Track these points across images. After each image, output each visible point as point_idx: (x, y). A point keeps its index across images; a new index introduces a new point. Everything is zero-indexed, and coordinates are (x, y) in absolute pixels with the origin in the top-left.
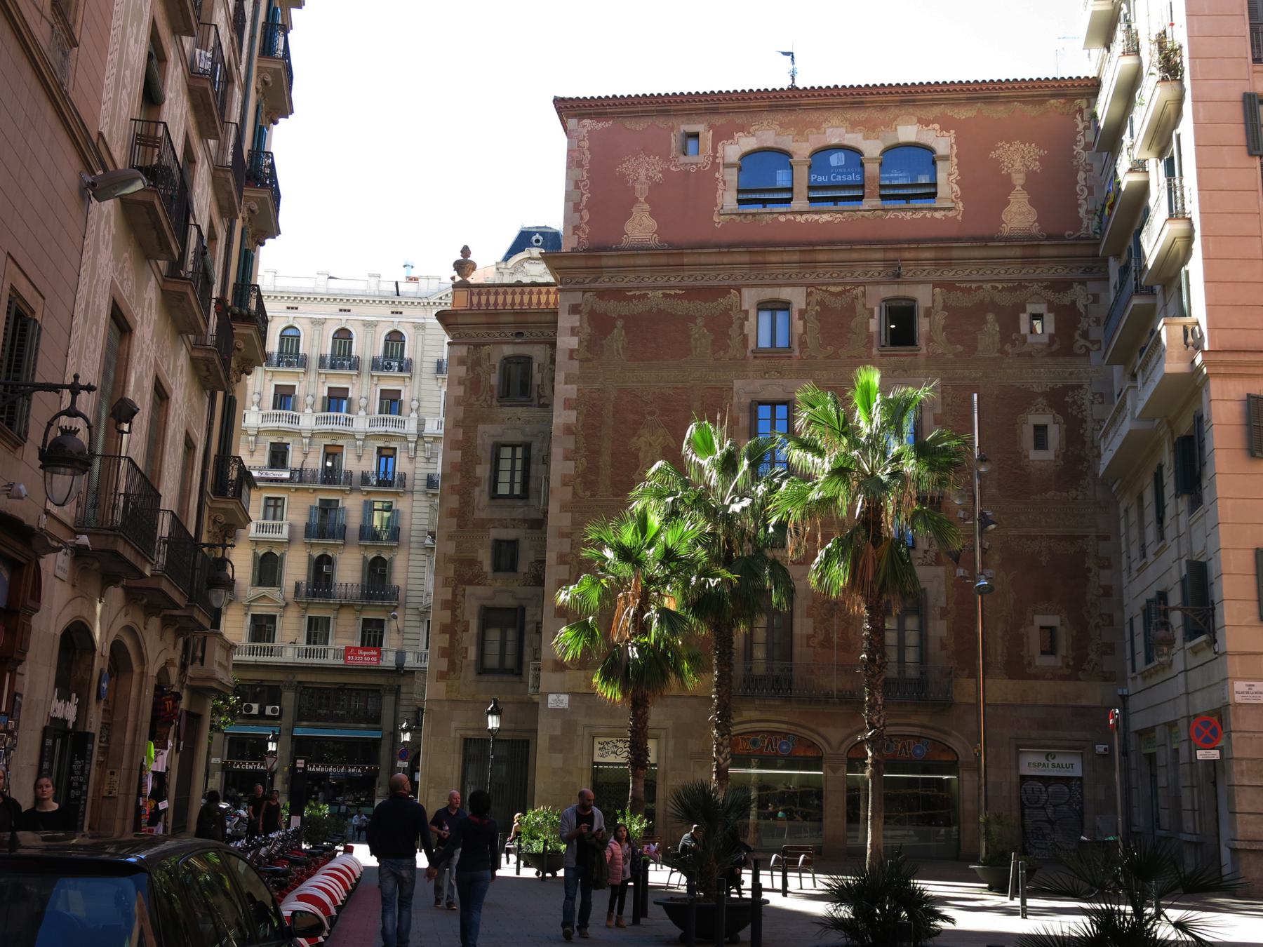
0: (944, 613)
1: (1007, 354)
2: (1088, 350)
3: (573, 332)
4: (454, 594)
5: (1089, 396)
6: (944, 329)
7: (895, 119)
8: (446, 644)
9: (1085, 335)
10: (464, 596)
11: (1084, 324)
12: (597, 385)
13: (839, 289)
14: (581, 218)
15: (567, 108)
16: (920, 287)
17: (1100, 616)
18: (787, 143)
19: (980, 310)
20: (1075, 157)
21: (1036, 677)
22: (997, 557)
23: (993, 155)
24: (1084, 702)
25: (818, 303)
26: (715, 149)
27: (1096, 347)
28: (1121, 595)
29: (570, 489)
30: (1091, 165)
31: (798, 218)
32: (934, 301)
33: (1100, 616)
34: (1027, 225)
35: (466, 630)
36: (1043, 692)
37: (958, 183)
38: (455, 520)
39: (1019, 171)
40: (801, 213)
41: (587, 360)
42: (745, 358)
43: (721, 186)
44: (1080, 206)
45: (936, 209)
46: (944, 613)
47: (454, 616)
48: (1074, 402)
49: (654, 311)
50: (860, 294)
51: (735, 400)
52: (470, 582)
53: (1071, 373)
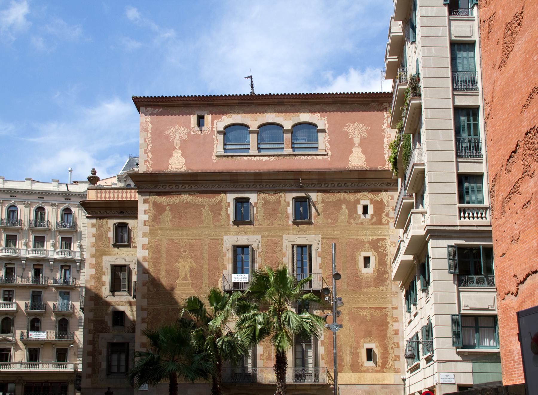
1: (351, 223)
2: (389, 222)
3: (146, 212)
4: (94, 337)
5: (389, 243)
8: (91, 361)
9: (387, 215)
10: (98, 338)
11: (387, 209)
12: (157, 238)
17: (394, 343)
21: (365, 371)
22: (347, 318)
24: (386, 382)
25: (263, 199)
28: (403, 333)
29: (146, 288)
31: (253, 158)
32: (317, 198)
33: (394, 343)
34: (361, 163)
35: (100, 354)
36: (369, 378)
37: (329, 142)
38: (93, 302)
39: (357, 137)
40: (255, 156)
41: (153, 226)
42: (228, 225)
47: (94, 348)
48: (382, 246)
49: (185, 202)
51: (225, 245)
52: (101, 332)
53: (381, 233)
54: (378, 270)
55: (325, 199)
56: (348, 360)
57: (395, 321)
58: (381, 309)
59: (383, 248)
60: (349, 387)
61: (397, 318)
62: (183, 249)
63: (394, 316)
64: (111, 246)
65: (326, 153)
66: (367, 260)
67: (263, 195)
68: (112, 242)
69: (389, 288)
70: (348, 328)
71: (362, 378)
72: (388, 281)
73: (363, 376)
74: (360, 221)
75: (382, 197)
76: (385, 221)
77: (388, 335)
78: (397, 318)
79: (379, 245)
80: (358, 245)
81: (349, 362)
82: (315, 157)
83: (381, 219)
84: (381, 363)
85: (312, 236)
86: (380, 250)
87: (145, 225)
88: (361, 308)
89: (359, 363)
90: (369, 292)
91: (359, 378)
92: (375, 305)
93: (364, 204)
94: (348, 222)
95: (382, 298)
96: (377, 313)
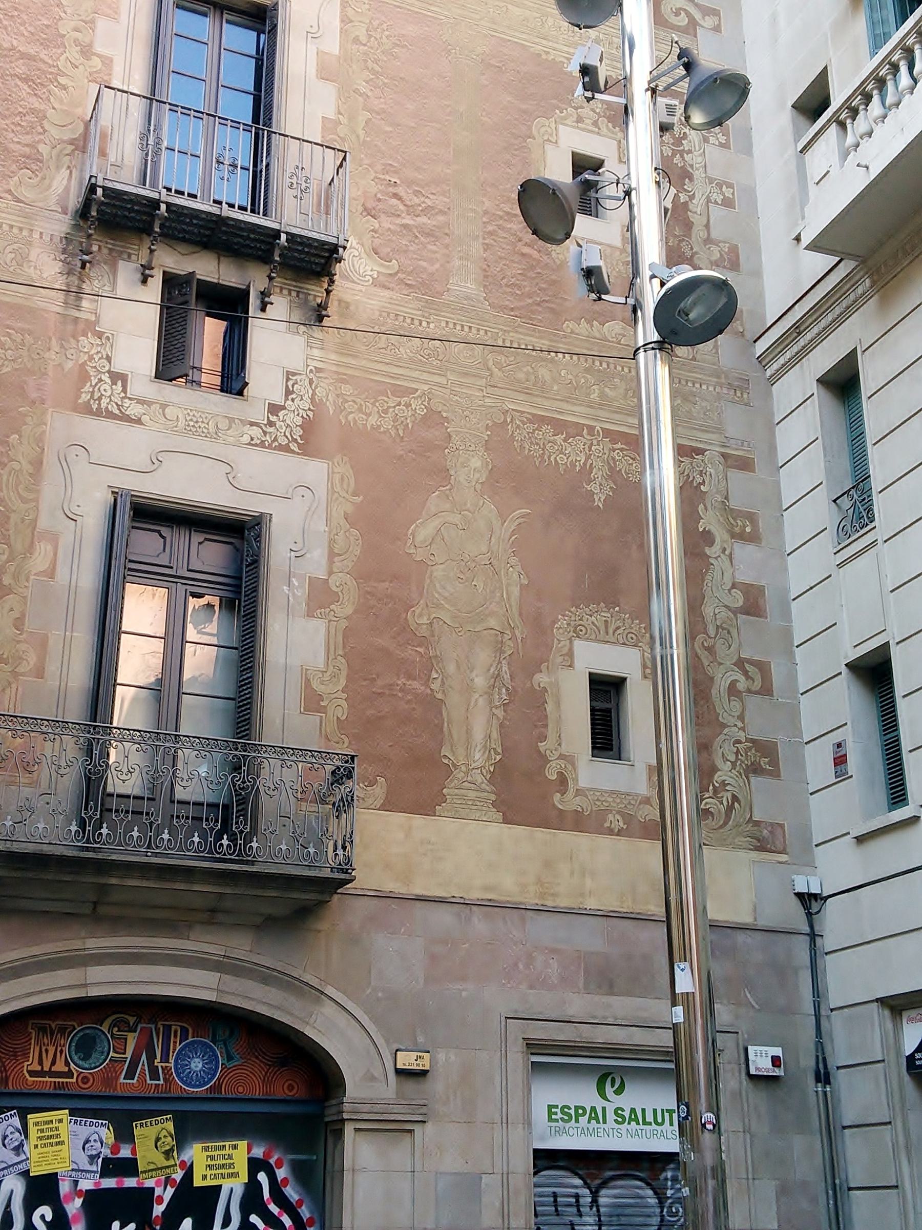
0: (320, 597)
17: (740, 664)
21: (578, 822)
22: (476, 463)
27: (709, 22)
33: (740, 664)
46: (320, 597)
56: (479, 734)
57: (742, 537)
60: (479, 924)
63: (734, 504)
78: (752, 517)
88: (559, 426)
89: (544, 759)
91: (548, 864)
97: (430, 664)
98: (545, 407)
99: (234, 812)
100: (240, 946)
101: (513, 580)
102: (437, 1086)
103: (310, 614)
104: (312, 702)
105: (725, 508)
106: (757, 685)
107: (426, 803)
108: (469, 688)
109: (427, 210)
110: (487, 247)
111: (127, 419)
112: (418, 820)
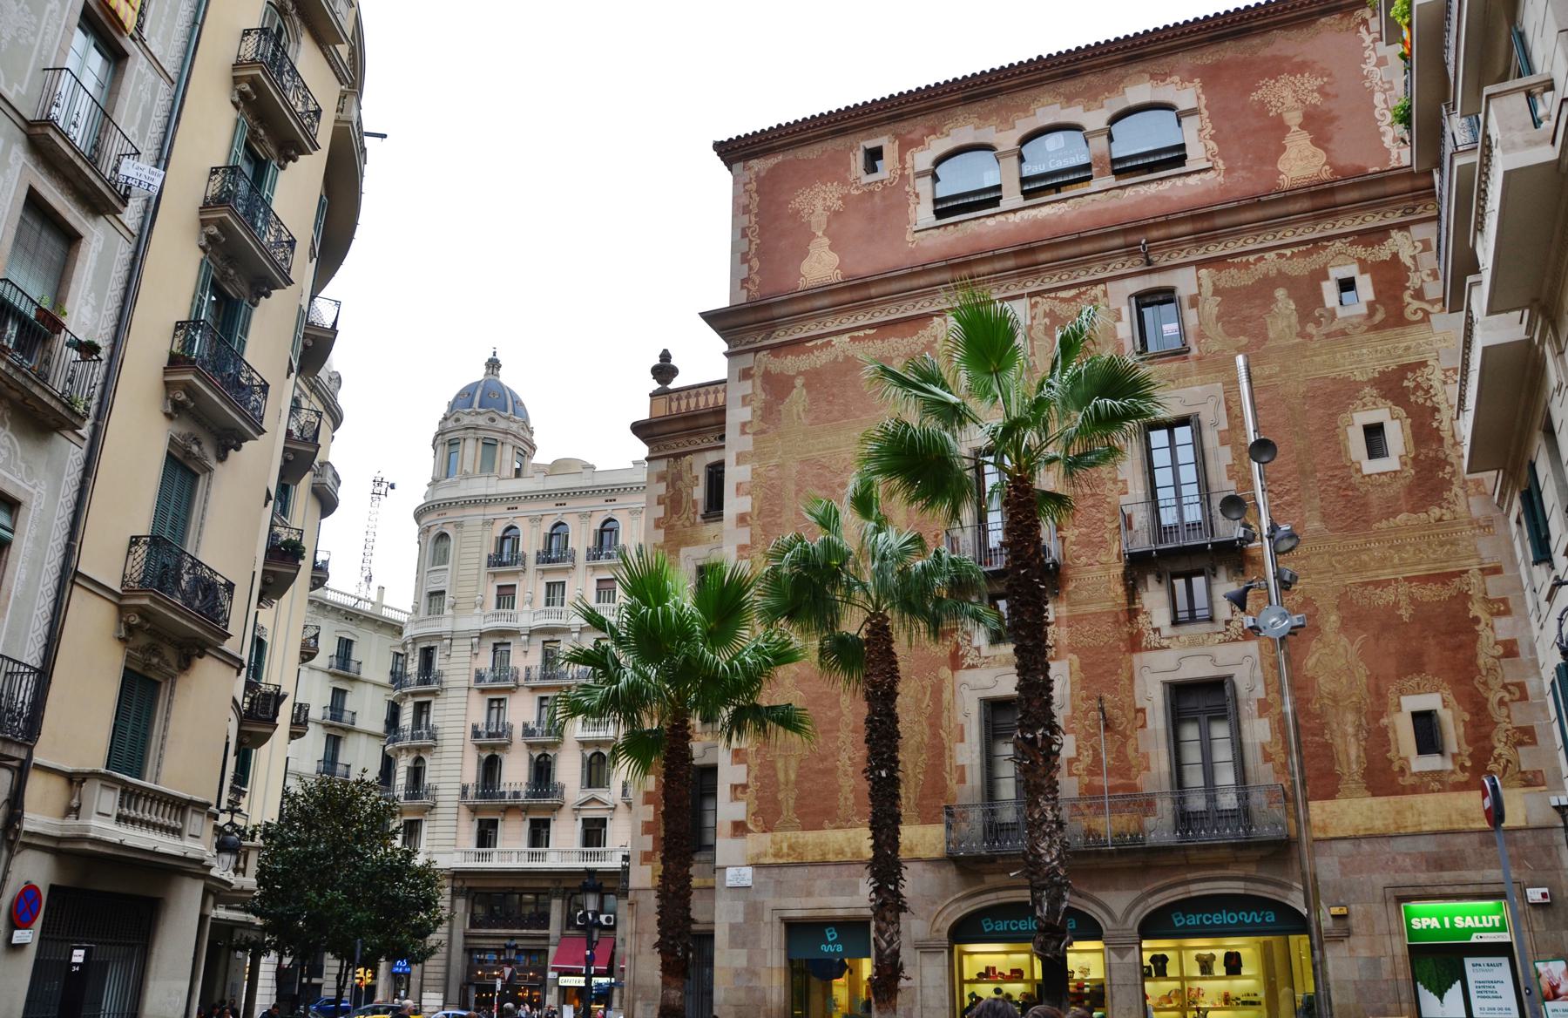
0: (1264, 707)
1: (1311, 337)
2: (1427, 313)
3: (745, 401)
5: (1439, 375)
6: (1219, 318)
7: (1121, 81)
9: (1419, 294)
11: (1414, 280)
12: (773, 462)
13: (1073, 292)
14: (750, 268)
15: (732, 151)
16: (1179, 272)
18: (988, 135)
19: (1263, 290)
20: (1366, 77)
21: (1414, 790)
22: (1333, 618)
23: (1255, 96)
25: (1046, 315)
26: (902, 160)
28: (1533, 650)
30: (1390, 82)
31: (1011, 217)
32: (1200, 286)
33: (1505, 687)
34: (1315, 170)
36: (1432, 810)
37: (1212, 138)
40: (1014, 211)
41: (763, 432)
43: (912, 199)
44: (1383, 134)
45: (1188, 174)
46: (1264, 707)
48: (1418, 386)
50: (1100, 294)
53: (1407, 348)
54: (1415, 459)
55: (1221, 284)
56: (1353, 757)
57: (1499, 614)
58: (1444, 578)
59: (1420, 393)
60: (1366, 847)
61: (1504, 601)
62: (838, 480)
63: (1490, 596)
64: (699, 519)
65: (1209, 165)
66: (1374, 433)
67: (1044, 304)
68: (701, 510)
69: (1461, 508)
70: (1341, 650)
71: (1408, 814)
72: (1455, 489)
73: (1412, 807)
74: (1335, 326)
75: (1395, 249)
76: (1415, 312)
77: (1481, 662)
78: (1504, 601)
79: (1406, 383)
80: (1342, 394)
81: (1359, 763)
82: (1179, 182)
83: (1401, 307)
84: (1471, 756)
85: (1197, 389)
86: (1413, 399)
87: (743, 432)
88: (1377, 584)
89: (1391, 762)
90: (1397, 529)
91: (1398, 812)
92: (1422, 569)
93: (1341, 277)
94: (1298, 335)
95: (1442, 544)
96: (1429, 593)
97: (1324, 726)
98: (1369, 575)
99: (1244, 813)
100: (1252, 870)
101: (1362, 671)
102: (1353, 921)
103: (1260, 716)
104: (1267, 758)
105: (1486, 600)
106: (1518, 695)
107: (1331, 795)
108: (1345, 735)
109: (1288, 492)
110: (1322, 500)
111: (1163, 648)
112: (1328, 803)
